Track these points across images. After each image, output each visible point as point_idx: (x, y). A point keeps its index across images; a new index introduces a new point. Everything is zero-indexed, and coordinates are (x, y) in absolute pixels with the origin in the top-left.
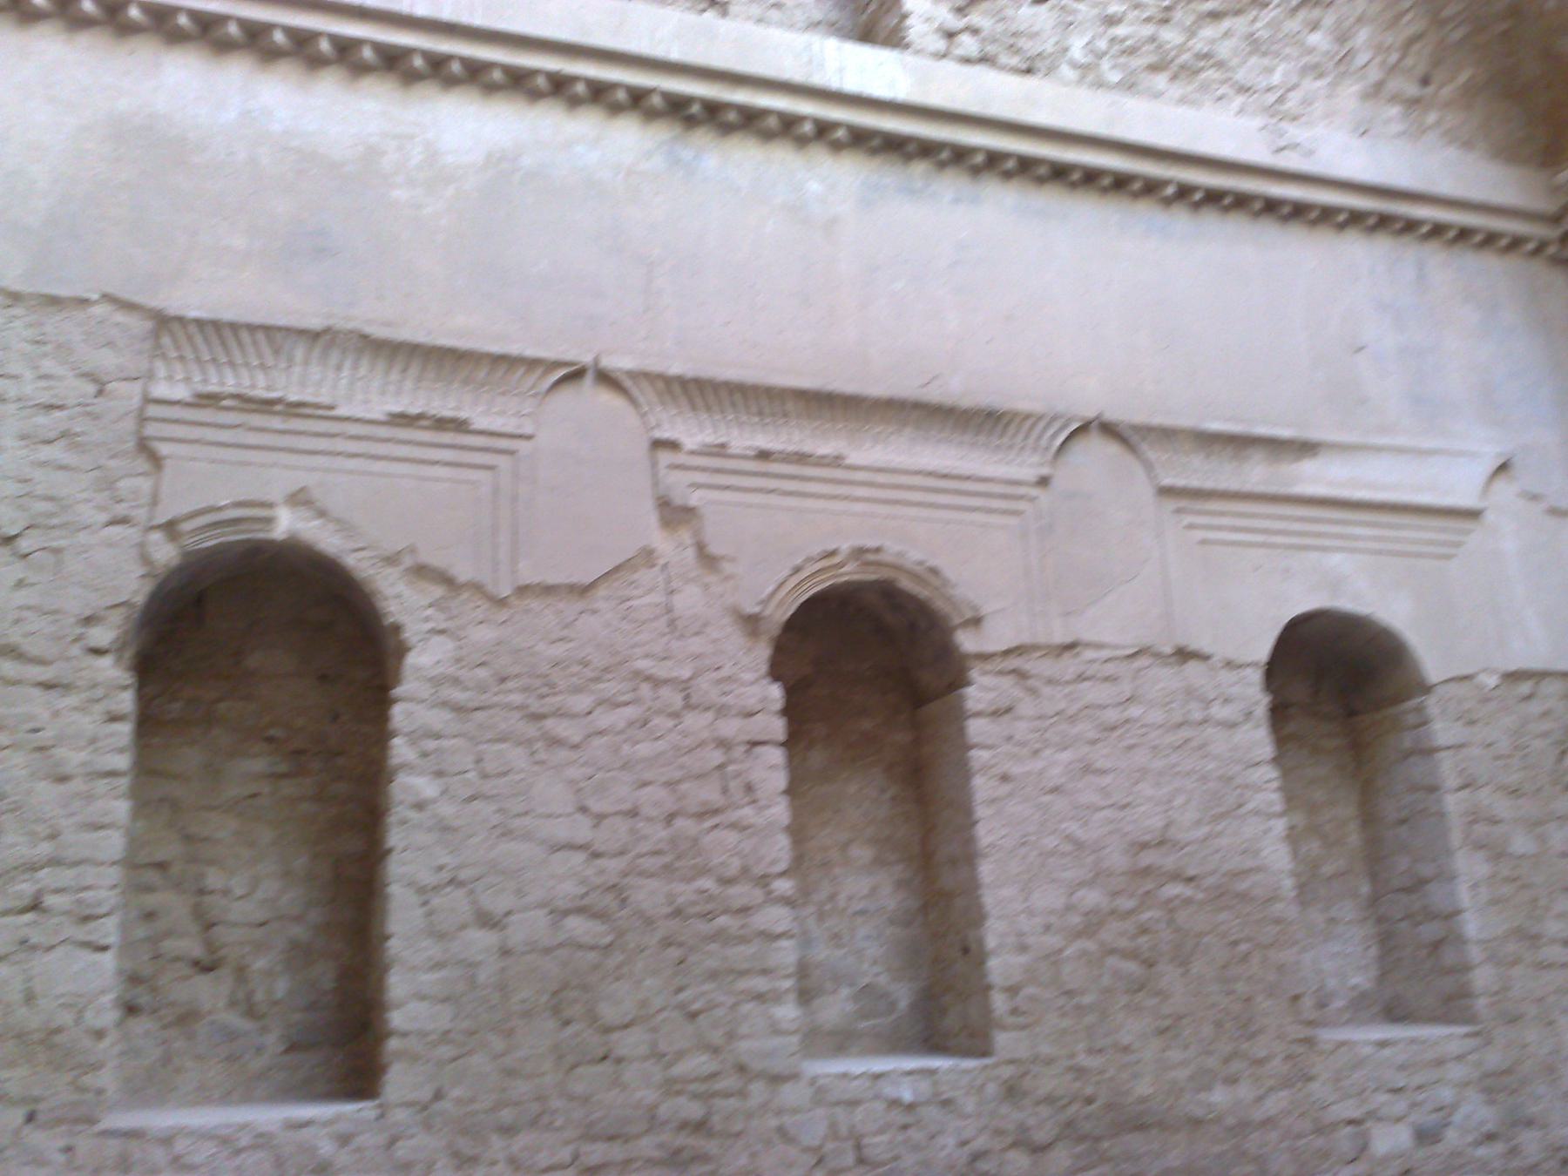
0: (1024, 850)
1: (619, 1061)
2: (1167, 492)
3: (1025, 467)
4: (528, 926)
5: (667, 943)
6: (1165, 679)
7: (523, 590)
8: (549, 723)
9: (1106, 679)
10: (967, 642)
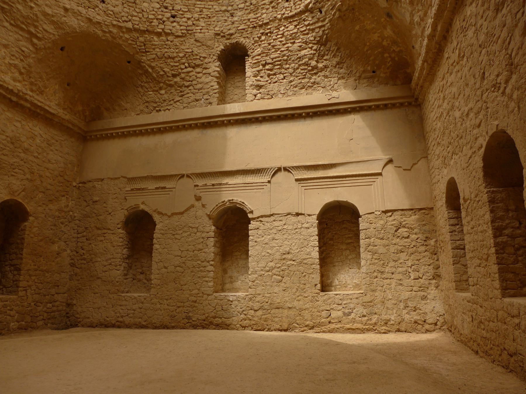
0: (258, 255)
1: (183, 290)
2: (297, 180)
3: (266, 179)
4: (171, 268)
5: (192, 272)
6: (294, 219)
7: (173, 214)
8: (175, 236)
9: (280, 221)
10: (250, 216)
